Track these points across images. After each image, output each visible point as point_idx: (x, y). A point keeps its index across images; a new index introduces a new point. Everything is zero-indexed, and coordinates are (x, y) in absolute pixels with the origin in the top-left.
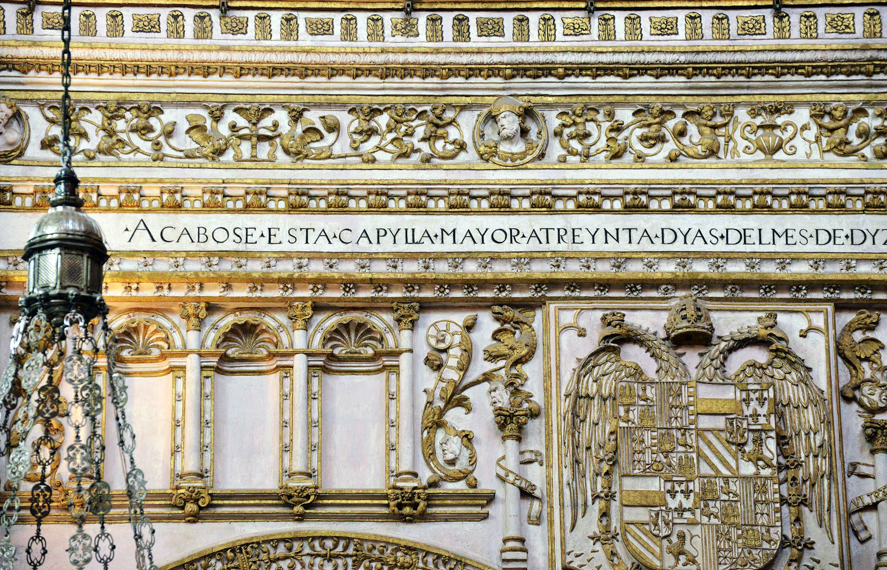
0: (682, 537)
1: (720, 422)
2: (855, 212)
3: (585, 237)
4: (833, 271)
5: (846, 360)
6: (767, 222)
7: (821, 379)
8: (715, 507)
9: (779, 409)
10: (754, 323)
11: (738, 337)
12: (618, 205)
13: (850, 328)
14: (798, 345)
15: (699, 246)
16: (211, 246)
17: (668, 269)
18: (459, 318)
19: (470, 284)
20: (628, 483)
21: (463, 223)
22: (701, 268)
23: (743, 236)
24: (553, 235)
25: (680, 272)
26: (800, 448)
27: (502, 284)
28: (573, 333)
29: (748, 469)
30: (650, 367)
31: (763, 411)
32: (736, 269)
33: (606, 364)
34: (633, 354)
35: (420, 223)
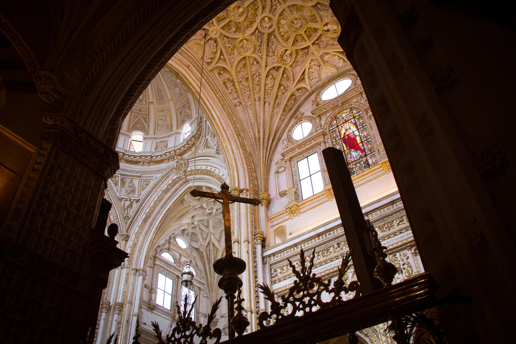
2: (387, 239)
21: (333, 263)
28: (351, 273)
35: (327, 265)
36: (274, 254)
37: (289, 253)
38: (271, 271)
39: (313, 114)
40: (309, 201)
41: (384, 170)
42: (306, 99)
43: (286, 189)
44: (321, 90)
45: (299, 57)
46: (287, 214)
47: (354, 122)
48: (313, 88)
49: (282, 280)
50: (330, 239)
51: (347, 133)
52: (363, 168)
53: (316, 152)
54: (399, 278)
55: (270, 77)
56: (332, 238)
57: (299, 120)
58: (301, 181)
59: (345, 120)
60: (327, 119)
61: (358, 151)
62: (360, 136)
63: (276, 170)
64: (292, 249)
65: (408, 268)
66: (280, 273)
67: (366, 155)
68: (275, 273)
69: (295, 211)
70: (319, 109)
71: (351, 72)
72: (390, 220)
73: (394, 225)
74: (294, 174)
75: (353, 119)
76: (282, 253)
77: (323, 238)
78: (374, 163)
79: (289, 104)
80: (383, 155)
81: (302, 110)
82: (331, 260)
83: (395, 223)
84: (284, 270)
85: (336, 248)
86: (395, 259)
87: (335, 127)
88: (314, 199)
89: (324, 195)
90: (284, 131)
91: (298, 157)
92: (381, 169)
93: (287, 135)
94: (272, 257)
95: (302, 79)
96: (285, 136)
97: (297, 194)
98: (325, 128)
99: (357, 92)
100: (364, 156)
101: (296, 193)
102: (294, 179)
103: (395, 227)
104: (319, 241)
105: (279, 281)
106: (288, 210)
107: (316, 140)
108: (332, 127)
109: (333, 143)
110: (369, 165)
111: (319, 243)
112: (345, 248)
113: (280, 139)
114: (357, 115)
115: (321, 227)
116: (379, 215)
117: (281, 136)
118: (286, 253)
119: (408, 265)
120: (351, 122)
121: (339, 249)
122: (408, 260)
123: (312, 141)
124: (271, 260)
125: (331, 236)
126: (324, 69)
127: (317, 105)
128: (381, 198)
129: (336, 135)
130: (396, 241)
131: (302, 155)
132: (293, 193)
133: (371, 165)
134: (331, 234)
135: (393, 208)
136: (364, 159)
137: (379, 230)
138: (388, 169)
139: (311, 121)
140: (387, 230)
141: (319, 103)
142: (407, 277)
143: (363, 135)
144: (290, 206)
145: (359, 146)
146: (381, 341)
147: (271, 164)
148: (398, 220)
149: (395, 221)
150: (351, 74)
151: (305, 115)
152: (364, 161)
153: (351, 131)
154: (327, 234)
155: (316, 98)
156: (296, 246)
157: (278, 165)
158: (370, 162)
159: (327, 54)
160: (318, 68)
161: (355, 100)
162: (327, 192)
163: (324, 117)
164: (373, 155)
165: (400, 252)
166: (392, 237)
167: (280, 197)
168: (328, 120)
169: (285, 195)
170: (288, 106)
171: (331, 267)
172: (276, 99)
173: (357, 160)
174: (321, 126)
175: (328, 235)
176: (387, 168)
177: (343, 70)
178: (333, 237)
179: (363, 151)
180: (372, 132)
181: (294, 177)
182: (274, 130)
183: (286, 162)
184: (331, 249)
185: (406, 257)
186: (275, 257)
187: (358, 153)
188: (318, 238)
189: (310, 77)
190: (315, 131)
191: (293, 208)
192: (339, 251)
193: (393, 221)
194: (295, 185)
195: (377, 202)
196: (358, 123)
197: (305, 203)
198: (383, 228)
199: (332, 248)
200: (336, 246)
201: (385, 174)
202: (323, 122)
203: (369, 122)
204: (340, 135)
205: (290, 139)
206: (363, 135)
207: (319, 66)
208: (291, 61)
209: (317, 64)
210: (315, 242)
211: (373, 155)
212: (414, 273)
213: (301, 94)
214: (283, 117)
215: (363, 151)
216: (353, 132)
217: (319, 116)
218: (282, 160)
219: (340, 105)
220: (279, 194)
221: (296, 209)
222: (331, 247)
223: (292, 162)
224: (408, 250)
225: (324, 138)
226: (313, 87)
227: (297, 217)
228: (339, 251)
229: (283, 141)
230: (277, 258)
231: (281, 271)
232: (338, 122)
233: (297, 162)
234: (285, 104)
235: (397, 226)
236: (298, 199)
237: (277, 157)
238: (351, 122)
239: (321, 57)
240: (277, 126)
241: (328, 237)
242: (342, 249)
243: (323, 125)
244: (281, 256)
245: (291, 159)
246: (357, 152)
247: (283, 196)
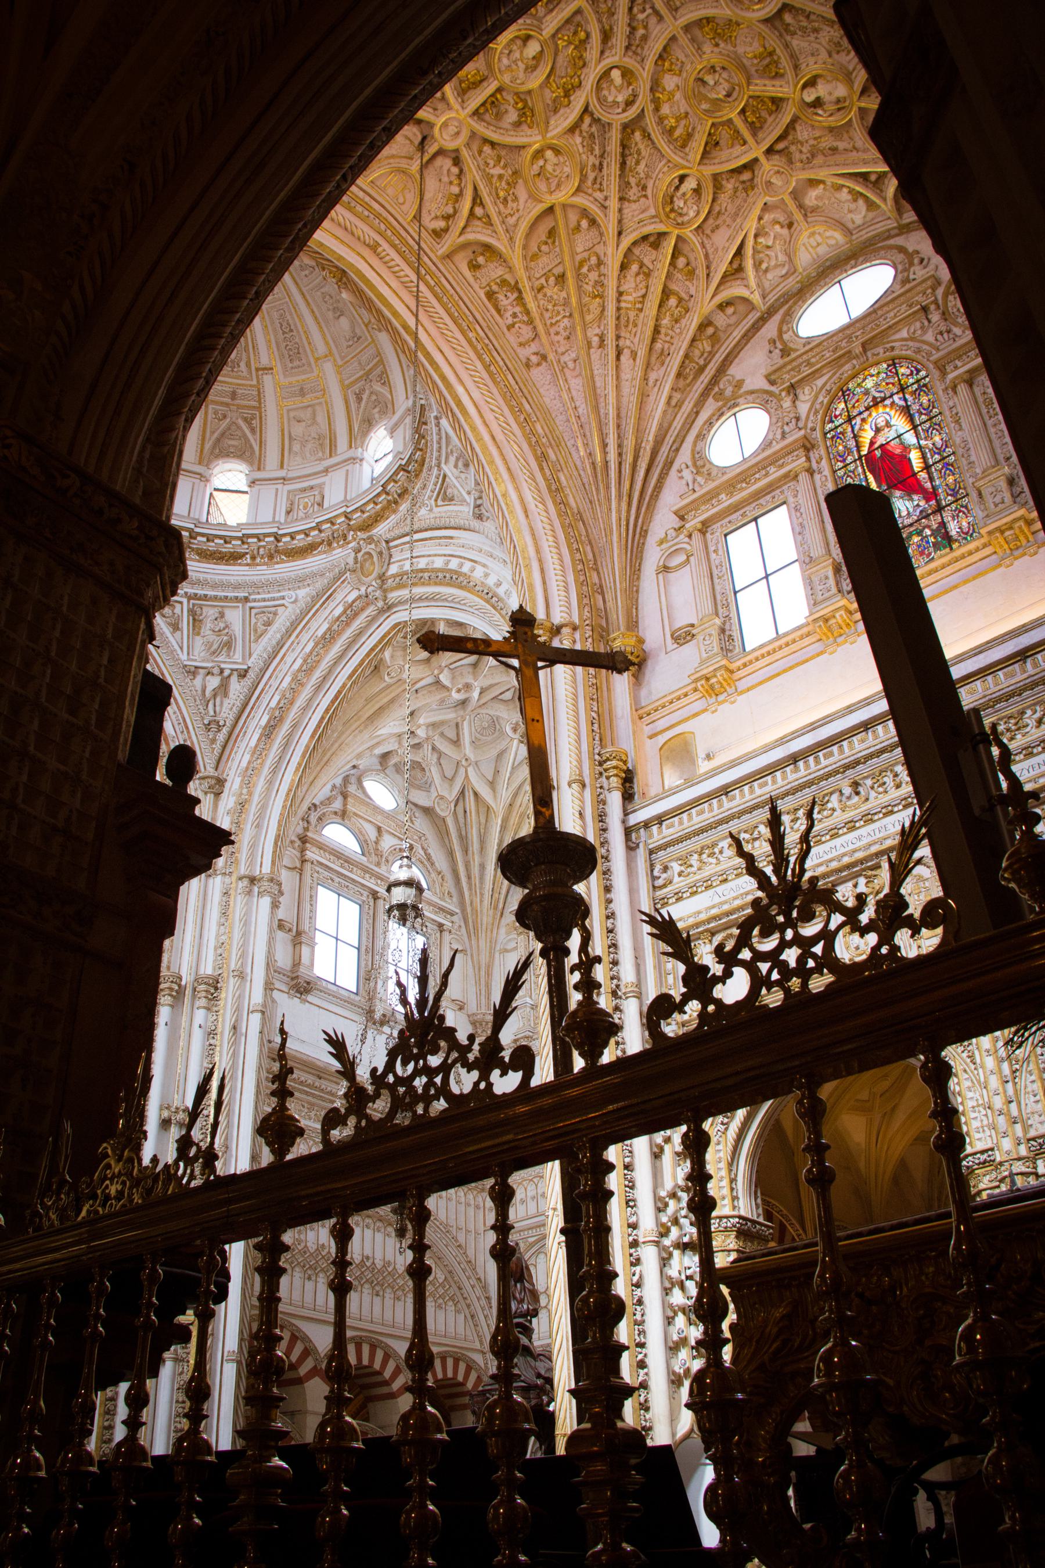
12: (901, 807)
16: (742, 891)
18: (850, 884)
19: (848, 867)
21: (838, 842)
24: (877, 831)
27: (861, 861)
36: (660, 819)
37: (706, 815)
38: (652, 871)
39: (772, 383)
40: (763, 656)
41: (995, 552)
42: (748, 336)
43: (695, 621)
44: (795, 303)
45: (724, 198)
46: (698, 695)
47: (902, 403)
48: (771, 298)
49: (685, 895)
50: (830, 768)
51: (881, 440)
52: (931, 549)
53: (784, 503)
55: (635, 268)
56: (834, 766)
57: (729, 404)
58: (738, 595)
59: (874, 398)
60: (816, 397)
61: (915, 497)
62: (920, 447)
63: (661, 563)
64: (715, 801)
66: (680, 875)
67: (939, 509)
68: (664, 876)
69: (722, 686)
70: (789, 367)
71: (892, 242)
72: (1013, 710)
73: (1028, 725)
74: (715, 572)
75: (897, 393)
76: (685, 815)
77: (807, 767)
78: (967, 534)
79: (697, 353)
80: (992, 506)
81: (735, 371)
82: (833, 832)
83: (1029, 718)
84: (691, 866)
85: (849, 798)
87: (841, 421)
88: (780, 648)
89: (808, 635)
90: (681, 439)
91: (727, 520)
92: (988, 551)
93: (693, 451)
94: (655, 829)
95: (735, 271)
96: (685, 455)
97: (727, 633)
98: (810, 425)
99: (911, 306)
100: (934, 513)
101: (723, 631)
102: (718, 588)
103: (1028, 729)
104: (795, 776)
105: (678, 900)
106: (699, 684)
107: (782, 466)
108: (833, 422)
109: (834, 472)
110: (948, 539)
111: (796, 783)
113: (669, 464)
114: (911, 381)
115: (803, 734)
116: (981, 696)
117: (672, 454)
118: (698, 815)
120: (893, 403)
121: (856, 799)
123: (772, 469)
124: (651, 836)
125: (832, 760)
126: (806, 234)
127: (785, 352)
128: (988, 642)
129: (845, 447)
130: (1032, 773)
131: (741, 512)
132: (715, 632)
133: (956, 540)
134: (831, 754)
135: (1025, 672)
136: (934, 521)
138: (1008, 551)
139: (764, 406)
141: (791, 345)
143: (929, 443)
144: (705, 672)
145: (918, 480)
146: (980, 1070)
147: (643, 544)
148: (1038, 708)
149: (1029, 712)
150: (890, 247)
151: (748, 386)
152: (935, 527)
153: (892, 434)
154: (821, 754)
155: (780, 333)
156: (726, 794)
157: (664, 546)
158: (953, 528)
159: (813, 183)
160: (785, 232)
161: (904, 334)
162: (820, 626)
163: (807, 390)
164: (962, 506)
166: (1020, 761)
167: (676, 646)
168: (821, 398)
169: (689, 638)
170: (692, 361)
171: (835, 854)
172: (653, 340)
173: (911, 525)
174: (798, 419)
175: (822, 759)
176: (1006, 546)
177: (865, 235)
178: (838, 765)
179: (931, 495)
180: (960, 433)
181: (716, 581)
182: (651, 438)
183: (690, 536)
184: (834, 801)
186: (664, 826)
187: (915, 503)
188: (792, 766)
189: (760, 263)
190: (779, 436)
191: (715, 676)
192: (856, 807)
193: (1023, 713)
194: (719, 607)
195: (975, 655)
196: (915, 408)
197: (751, 662)
199: (835, 798)
200: (847, 791)
201: (999, 566)
202: (803, 408)
203: (951, 404)
204: (858, 447)
205: (700, 464)
206: (929, 443)
207: (790, 225)
208: (698, 213)
209: (782, 219)
210: (783, 779)
211: (962, 506)
213: (733, 320)
214: (677, 396)
215: (931, 495)
216: (899, 436)
217: (792, 389)
218: (678, 530)
219: (858, 350)
220: (672, 636)
221: (724, 680)
222: (831, 793)
223: (708, 535)
225: (808, 459)
226: (770, 296)
227: (726, 705)
228: (856, 807)
229: (680, 471)
230: (671, 831)
231: (682, 868)
232: (850, 406)
233: (726, 536)
234: (681, 353)
235: (1038, 727)
236: (731, 651)
237: (663, 522)
238: (893, 403)
239: (796, 195)
240: (661, 425)
241: (824, 762)
242: (867, 799)
243: (803, 416)
244: (681, 823)
245: (704, 528)
246: (912, 500)
247: (682, 641)
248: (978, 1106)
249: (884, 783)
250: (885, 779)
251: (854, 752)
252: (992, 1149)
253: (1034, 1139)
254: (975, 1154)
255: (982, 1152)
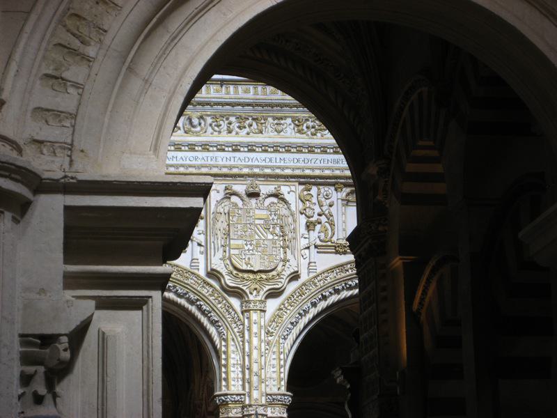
0: (249, 259)
1: (262, 222)
2: (305, 153)
3: (220, 159)
4: (298, 172)
5: (302, 201)
6: (278, 156)
7: (293, 208)
8: (259, 249)
9: (280, 217)
10: (273, 189)
11: (268, 193)
13: (303, 190)
14: (287, 197)
15: (256, 163)
17: (246, 171)
20: (232, 242)
22: (257, 171)
23: (271, 160)
24: (209, 159)
25: (250, 172)
26: (286, 229)
29: (270, 237)
30: (240, 203)
31: (276, 218)
32: (268, 171)
33: (226, 202)
34: (234, 199)
54: (307, 236)
65: (327, 225)
82: (178, 146)
85: (194, 127)
86: (308, 198)
112: (212, 134)
119: (328, 219)
122: (331, 209)
130: (322, 165)
137: (293, 126)
140: (309, 133)
142: (321, 241)
165: (321, 187)
166: (317, 153)
185: (328, 201)
198: (303, 125)
212: (334, 239)
224: (336, 190)
228: (197, 134)
248: (237, 364)
249: (220, 125)
250: (221, 122)
251: (209, 96)
252: (244, 395)
253: (271, 395)
254: (233, 395)
255: (237, 395)
